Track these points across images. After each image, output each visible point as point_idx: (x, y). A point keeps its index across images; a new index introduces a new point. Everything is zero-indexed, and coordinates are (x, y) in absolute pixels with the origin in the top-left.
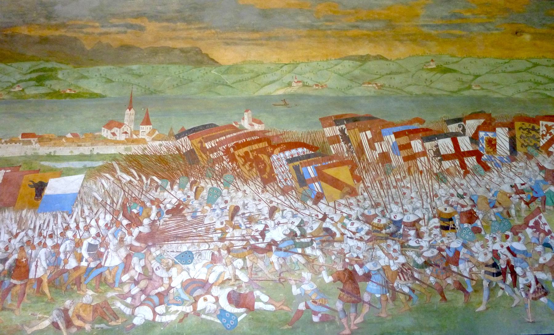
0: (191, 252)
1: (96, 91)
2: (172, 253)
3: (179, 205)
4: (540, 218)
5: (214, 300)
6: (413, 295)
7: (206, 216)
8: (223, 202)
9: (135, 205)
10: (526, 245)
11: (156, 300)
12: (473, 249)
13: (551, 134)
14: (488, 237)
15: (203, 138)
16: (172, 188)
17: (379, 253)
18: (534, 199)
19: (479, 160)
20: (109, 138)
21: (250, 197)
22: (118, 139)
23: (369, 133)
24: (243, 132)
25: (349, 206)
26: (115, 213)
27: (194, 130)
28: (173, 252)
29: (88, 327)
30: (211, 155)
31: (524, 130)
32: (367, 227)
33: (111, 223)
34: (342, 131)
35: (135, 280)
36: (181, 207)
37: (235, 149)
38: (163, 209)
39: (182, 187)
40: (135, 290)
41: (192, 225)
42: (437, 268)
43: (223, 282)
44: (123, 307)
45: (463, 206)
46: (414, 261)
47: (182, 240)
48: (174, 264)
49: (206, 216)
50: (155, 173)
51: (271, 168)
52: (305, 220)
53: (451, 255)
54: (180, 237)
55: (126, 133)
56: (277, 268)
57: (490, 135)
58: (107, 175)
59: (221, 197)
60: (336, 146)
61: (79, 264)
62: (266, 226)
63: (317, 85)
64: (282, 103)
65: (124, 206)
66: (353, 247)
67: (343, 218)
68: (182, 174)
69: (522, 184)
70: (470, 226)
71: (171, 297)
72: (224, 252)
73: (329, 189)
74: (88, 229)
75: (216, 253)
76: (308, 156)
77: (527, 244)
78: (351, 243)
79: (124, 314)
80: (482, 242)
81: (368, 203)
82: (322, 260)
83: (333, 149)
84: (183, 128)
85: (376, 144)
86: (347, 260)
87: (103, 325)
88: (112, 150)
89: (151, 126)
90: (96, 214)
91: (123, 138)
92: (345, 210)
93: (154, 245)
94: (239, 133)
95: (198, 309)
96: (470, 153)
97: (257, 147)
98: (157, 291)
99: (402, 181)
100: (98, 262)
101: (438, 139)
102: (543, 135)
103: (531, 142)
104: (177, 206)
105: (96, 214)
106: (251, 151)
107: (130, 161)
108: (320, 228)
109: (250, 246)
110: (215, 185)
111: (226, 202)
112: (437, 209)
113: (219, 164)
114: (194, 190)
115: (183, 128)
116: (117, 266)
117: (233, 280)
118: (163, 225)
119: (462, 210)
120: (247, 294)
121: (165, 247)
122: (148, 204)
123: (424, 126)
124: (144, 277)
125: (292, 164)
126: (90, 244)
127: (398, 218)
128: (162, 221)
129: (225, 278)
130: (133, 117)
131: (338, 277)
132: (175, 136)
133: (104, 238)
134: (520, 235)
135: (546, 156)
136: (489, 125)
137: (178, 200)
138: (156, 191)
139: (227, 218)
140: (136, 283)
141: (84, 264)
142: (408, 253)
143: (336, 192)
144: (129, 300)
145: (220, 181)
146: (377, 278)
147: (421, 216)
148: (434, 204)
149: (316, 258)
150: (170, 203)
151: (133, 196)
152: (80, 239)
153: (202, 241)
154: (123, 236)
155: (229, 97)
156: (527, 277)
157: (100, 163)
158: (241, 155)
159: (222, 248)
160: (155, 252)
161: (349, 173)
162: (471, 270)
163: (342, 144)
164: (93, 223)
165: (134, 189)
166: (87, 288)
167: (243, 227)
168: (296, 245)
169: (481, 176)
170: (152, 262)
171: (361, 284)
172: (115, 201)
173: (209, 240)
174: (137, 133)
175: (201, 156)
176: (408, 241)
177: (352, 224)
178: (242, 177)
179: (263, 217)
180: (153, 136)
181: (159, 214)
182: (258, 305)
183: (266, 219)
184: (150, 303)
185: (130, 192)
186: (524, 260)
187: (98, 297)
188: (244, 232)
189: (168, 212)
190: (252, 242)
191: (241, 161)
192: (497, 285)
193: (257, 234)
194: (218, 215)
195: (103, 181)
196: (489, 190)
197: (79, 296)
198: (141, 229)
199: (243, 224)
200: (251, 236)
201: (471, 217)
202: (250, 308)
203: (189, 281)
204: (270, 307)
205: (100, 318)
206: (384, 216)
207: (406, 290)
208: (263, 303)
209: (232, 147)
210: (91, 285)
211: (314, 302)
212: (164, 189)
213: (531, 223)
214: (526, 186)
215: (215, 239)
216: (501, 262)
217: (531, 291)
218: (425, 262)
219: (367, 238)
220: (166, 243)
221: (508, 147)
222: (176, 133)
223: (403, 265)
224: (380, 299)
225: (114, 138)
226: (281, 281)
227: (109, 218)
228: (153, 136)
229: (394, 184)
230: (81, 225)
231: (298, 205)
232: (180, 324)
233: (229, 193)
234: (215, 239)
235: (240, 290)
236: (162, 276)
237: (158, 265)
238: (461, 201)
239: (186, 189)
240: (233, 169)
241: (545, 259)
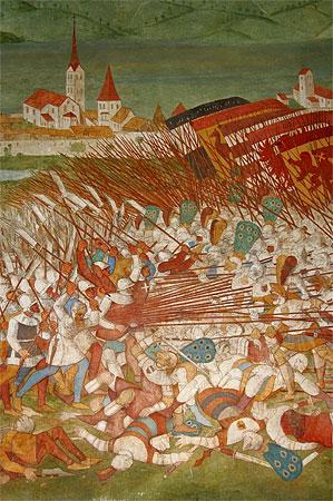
0: (210, 341)
2: (176, 343)
5: (257, 427)
7: (234, 275)
8: (264, 249)
9: (101, 254)
11: (151, 425)
15: (220, 127)
22: (56, 126)
26: (62, 268)
29: (29, 474)
30: (237, 160)
35: (109, 389)
37: (283, 149)
38: (153, 262)
39: (185, 221)
40: (112, 409)
41: (209, 291)
43: (273, 395)
44: (91, 438)
47: (192, 319)
48: (181, 362)
49: (234, 275)
50: (133, 194)
54: (189, 313)
55: (71, 115)
58: (42, 197)
61: (5, 361)
65: (79, 255)
68: (185, 196)
71: (179, 420)
72: (271, 341)
74: (16, 297)
75: (256, 342)
87: (57, 471)
88: (48, 149)
89: (119, 103)
90: (27, 271)
91: (66, 124)
93: (140, 327)
97: (326, 145)
98: (152, 410)
100: (40, 358)
105: (27, 271)
106: (314, 153)
110: (248, 218)
111: (270, 249)
113: (252, 178)
116: (74, 365)
117: (290, 392)
118: (155, 290)
120: (317, 418)
124: (127, 385)
128: (152, 283)
129: (276, 388)
130: (82, 83)
132: (167, 122)
133: (47, 314)
138: (138, 229)
139: (274, 279)
140: (114, 395)
141: (13, 361)
144: (102, 426)
145: (257, 210)
151: (96, 236)
154: (82, 311)
155: (269, 42)
157: (27, 174)
158: (295, 159)
160: (144, 339)
164: (25, 286)
167: (305, 296)
170: (139, 358)
174: (92, 116)
175: (218, 161)
178: (298, 203)
180: (125, 122)
184: (141, 431)
187: (43, 419)
188: (307, 305)
189: (163, 267)
191: (294, 171)
194: (256, 274)
197: (8, 419)
198: (114, 297)
200: (320, 313)
205: (52, 458)
209: (278, 143)
210: (30, 399)
212: (152, 224)
215: (254, 317)
227: (53, 277)
228: (125, 122)
232: (197, 468)
233: (274, 232)
234: (254, 317)
235: (304, 410)
239: (194, 224)
240: (281, 187)
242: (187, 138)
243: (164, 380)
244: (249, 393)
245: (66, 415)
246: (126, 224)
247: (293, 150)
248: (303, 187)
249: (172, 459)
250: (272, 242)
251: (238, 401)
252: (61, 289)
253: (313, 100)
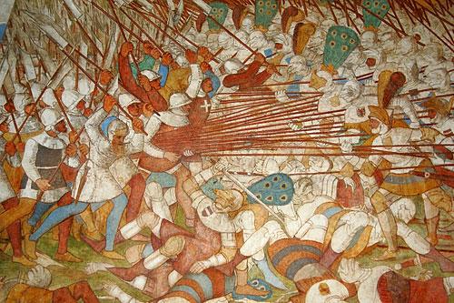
0: (287, 177)
2: (242, 178)
3: (256, 65)
5: (345, 292)
7: (323, 93)
9: (150, 61)
11: (205, 284)
16: (238, 27)
28: (244, 174)
35: (153, 235)
36: (262, 70)
38: (217, 73)
39: (261, 23)
40: (154, 260)
41: (289, 113)
43: (368, 251)
47: (263, 148)
48: (247, 203)
59: (357, 50)
65: (121, 61)
71: (241, 279)
72: (368, 181)
74: (37, 111)
75: (348, 181)
90: (54, 77)
93: (197, 156)
98: (207, 264)
100: (64, 190)
104: (250, 65)
109: (432, 171)
110: (343, 22)
111: (371, 62)
114: (292, 31)
116: (108, 201)
117: (391, 247)
118: (217, 110)
120: (426, 284)
121: (224, 163)
122: (181, 60)
128: (214, 100)
129: (373, 242)
133: (76, 134)
137: (254, 53)
139: (375, 101)
140: (158, 243)
141: (28, 193)
144: (140, 282)
145: (355, 12)
150: (233, 58)
152: (18, 134)
153: (312, 151)
154: (122, 132)
159: (363, 171)
160: (201, 172)
164: (48, 98)
165: (146, 22)
166: (36, 250)
167: (414, 123)
170: (194, 195)
172: (101, 49)
173: (332, 152)
181: (207, 84)
184: (192, 292)
185: (136, 30)
187: (64, 271)
188: (417, 136)
189: (230, 81)
190: (438, 161)
194: (351, 94)
197: (17, 268)
198: (165, 117)
199: (412, 117)
200: (434, 146)
203: (283, 245)
210: (46, 244)
212: (218, 26)
220: (227, 152)
227: (86, 88)
230: (19, 103)
233: (377, 41)
234: (345, 149)
235: (409, 273)
236: (219, 230)
237: (210, 203)
243: (224, 226)
244: (337, 246)
245: (94, 267)
246: (185, 24)
252: (96, 103)
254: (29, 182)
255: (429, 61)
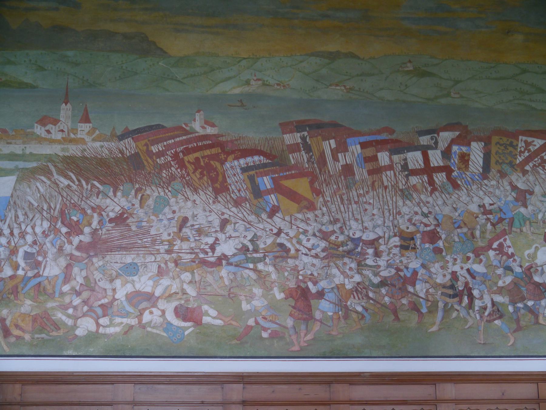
0: (136, 264)
1: (26, 80)
2: (116, 264)
3: (122, 214)
4: (505, 240)
5: (160, 313)
6: (366, 314)
7: (152, 226)
8: (171, 212)
9: (75, 212)
10: (486, 267)
11: (99, 311)
12: (433, 270)
13: (529, 151)
14: (448, 258)
15: (149, 141)
16: (115, 195)
17: (335, 271)
18: (501, 220)
19: (449, 177)
20: (43, 136)
21: (200, 208)
22: (53, 137)
23: (332, 142)
24: (193, 135)
25: (306, 221)
26: (52, 220)
27: (138, 131)
28: (117, 263)
29: (27, 337)
30: (158, 160)
31: (501, 145)
32: (323, 244)
33: (49, 230)
34: (303, 139)
35: (76, 291)
36: (125, 216)
37: (184, 155)
38: (105, 217)
39: (125, 195)
40: (77, 301)
42: (393, 289)
43: (170, 296)
44: (64, 318)
45: (426, 225)
46: (370, 280)
47: (126, 251)
48: (118, 276)
49: (152, 226)
50: (96, 178)
51: (224, 177)
52: (258, 234)
53: (408, 275)
54: (123, 247)
55: (62, 131)
56: (227, 283)
57: (464, 149)
58: (43, 178)
59: (168, 207)
60: (296, 155)
62: (217, 239)
63: (278, 85)
64: (239, 104)
65: (62, 212)
66: (307, 264)
67: (299, 233)
68: (126, 180)
69: (491, 205)
70: (431, 247)
71: (115, 309)
72: (171, 265)
73: (286, 203)
74: (24, 236)
75: (163, 265)
76: (265, 165)
77: (489, 266)
78: (305, 259)
79: (66, 325)
80: (442, 264)
81: (326, 219)
82: (274, 276)
83: (292, 158)
84: (127, 128)
85: (339, 155)
86: (300, 277)
87: (43, 335)
89: (91, 125)
90: (32, 220)
91: (59, 136)
92: (302, 225)
93: (96, 255)
94: (189, 136)
95: (144, 322)
96: (439, 169)
97: (209, 153)
98: (100, 303)
99: (364, 196)
101: (408, 151)
102: (521, 152)
103: (507, 159)
104: (120, 214)
105: (32, 220)
107: (68, 164)
108: (274, 243)
109: (199, 260)
110: (162, 194)
111: (174, 212)
112: (399, 228)
113: (166, 171)
114: (139, 198)
115: (127, 128)
116: (56, 276)
117: (180, 294)
118: (105, 234)
119: (425, 229)
120: (194, 309)
121: (108, 258)
122: (89, 211)
123: (394, 137)
124: (85, 288)
125: (247, 174)
126: (26, 252)
127: (357, 236)
128: (104, 230)
129: (173, 291)
130: (70, 113)
131: (290, 294)
132: (118, 137)
133: (41, 246)
134: (482, 257)
135: (521, 175)
136: (464, 139)
137: (122, 208)
138: (98, 198)
139: (175, 230)
140: (78, 294)
141: (20, 272)
142: (364, 272)
143: (294, 206)
144: (70, 311)
145: (168, 189)
146: (330, 296)
147: (381, 234)
148: (396, 222)
149: (269, 274)
150: (113, 210)
151: (72, 202)
152: (15, 246)
153: (148, 252)
154: (62, 245)
156: (484, 298)
157: (34, 164)
158: (191, 161)
159: (169, 260)
160: (97, 262)
161: (308, 185)
162: (427, 291)
163: (303, 153)
164: (29, 230)
165: (73, 194)
166: (25, 297)
167: (192, 240)
168: (247, 260)
169: (449, 194)
170: (95, 273)
171: (313, 302)
172: (53, 207)
173: (156, 252)
174: (75, 132)
175: (147, 161)
176: (365, 259)
177: (308, 240)
178: (192, 186)
179: (213, 230)
180: (94, 136)
181: (100, 222)
182: (206, 319)
183: (216, 231)
184: (93, 314)
185: (69, 198)
186: (483, 283)
188: (193, 245)
189: (111, 221)
190: (201, 256)
191: (191, 168)
192: (452, 306)
193: (207, 247)
194: (165, 226)
195: (38, 184)
196: (455, 209)
198: (82, 237)
199: (191, 236)
200: (200, 249)
201: (432, 237)
202: (198, 322)
204: (219, 322)
205: (41, 328)
206: (342, 233)
207: (360, 309)
208: (211, 317)
209: (182, 151)
211: (264, 318)
213: (495, 246)
214: (495, 206)
215: (162, 251)
216: (459, 283)
217: (486, 313)
218: (381, 281)
219: (323, 255)
220: (109, 253)
221: (481, 163)
222: (119, 133)
223: (358, 283)
224: (332, 318)
225: (49, 136)
226: (231, 296)
228: (94, 136)
229: (356, 199)
230: (16, 232)
231: (252, 218)
232: (125, 336)
233: (177, 202)
234: (162, 251)
235: (188, 304)
236: (106, 287)
237: (101, 276)
238: (425, 220)
239: (130, 196)
240: (182, 177)
241: (504, 282)
242: (129, 146)
243: (108, 286)
244: (157, 294)
246: (91, 195)
247: (191, 156)
248: (195, 177)
249: (111, 330)
250: (175, 208)
251: (150, 298)
252: (50, 232)
253: (203, 127)
254: (21, 268)
255: (199, 211)
